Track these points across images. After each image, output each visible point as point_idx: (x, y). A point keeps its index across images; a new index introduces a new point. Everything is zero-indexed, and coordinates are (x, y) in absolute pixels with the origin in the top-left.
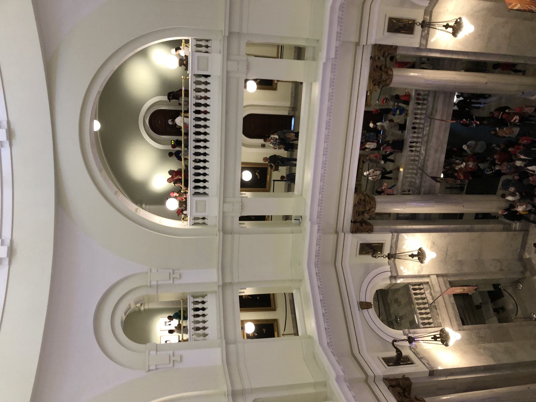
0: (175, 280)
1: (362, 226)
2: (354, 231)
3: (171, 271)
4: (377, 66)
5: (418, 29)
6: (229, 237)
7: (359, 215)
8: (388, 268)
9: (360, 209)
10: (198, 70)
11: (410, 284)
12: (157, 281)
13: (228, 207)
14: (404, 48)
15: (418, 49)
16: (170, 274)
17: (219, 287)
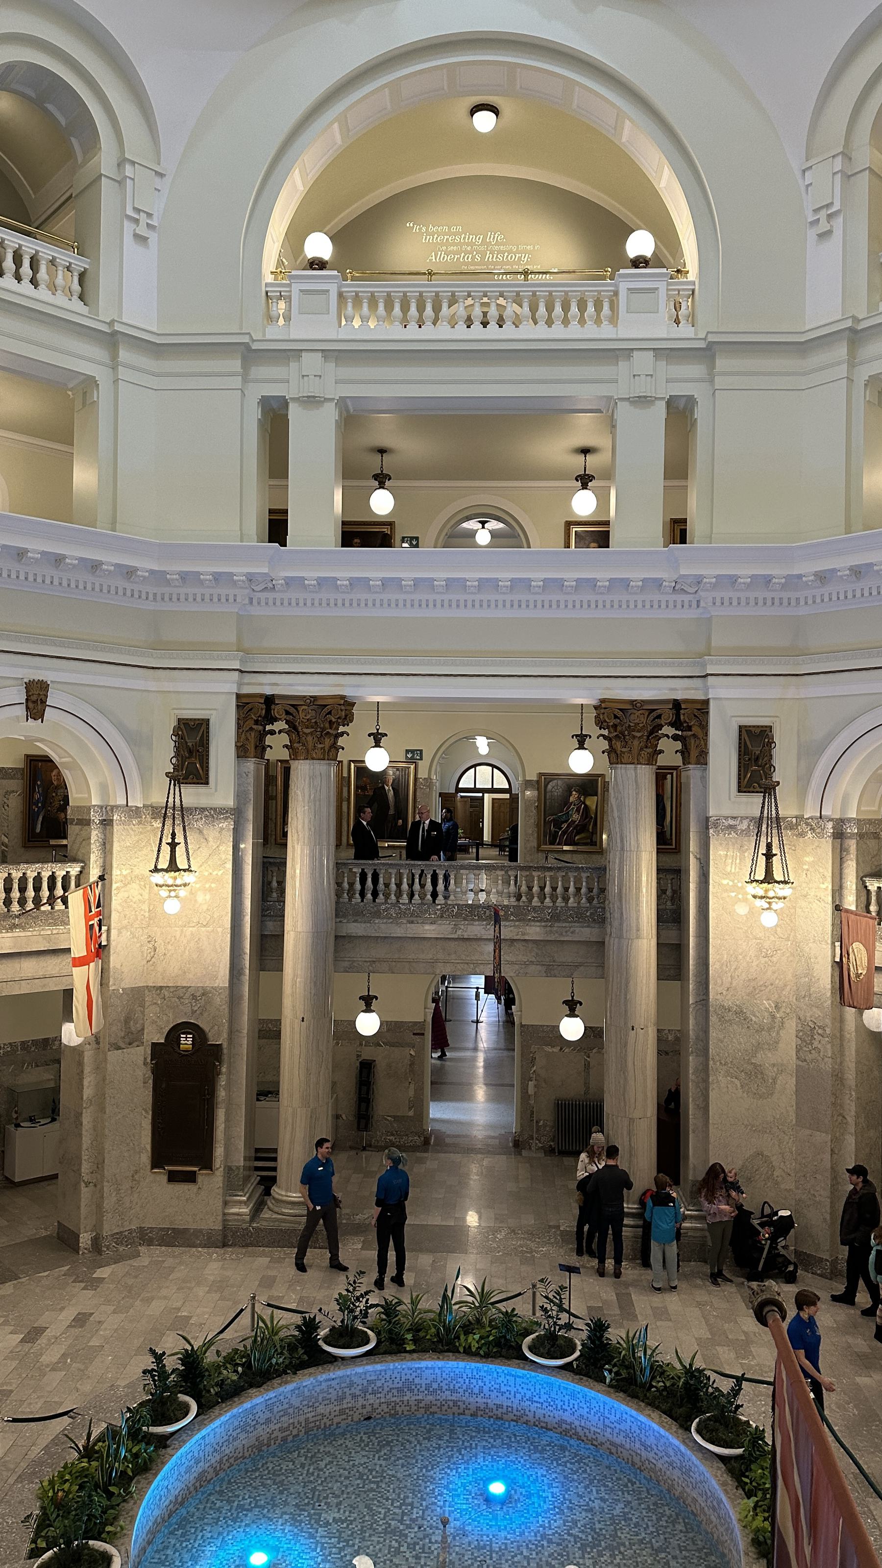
0: (133, 226)
1: (257, 722)
2: (244, 703)
3: (154, 223)
4: (659, 717)
5: (752, 804)
6: (235, 365)
7: (287, 713)
8: (137, 801)
9: (302, 715)
10: (629, 289)
11: (83, 867)
12: (133, 179)
13: (311, 363)
14: (704, 780)
15: (706, 824)
16: (149, 215)
17: (111, 323)
